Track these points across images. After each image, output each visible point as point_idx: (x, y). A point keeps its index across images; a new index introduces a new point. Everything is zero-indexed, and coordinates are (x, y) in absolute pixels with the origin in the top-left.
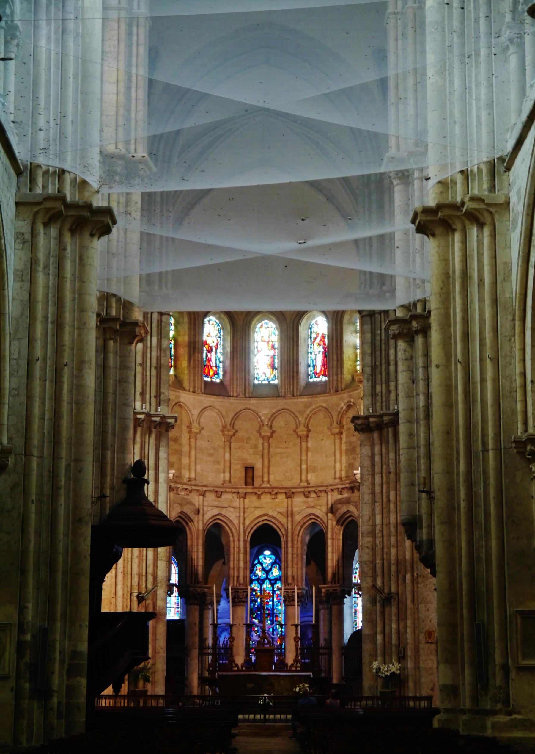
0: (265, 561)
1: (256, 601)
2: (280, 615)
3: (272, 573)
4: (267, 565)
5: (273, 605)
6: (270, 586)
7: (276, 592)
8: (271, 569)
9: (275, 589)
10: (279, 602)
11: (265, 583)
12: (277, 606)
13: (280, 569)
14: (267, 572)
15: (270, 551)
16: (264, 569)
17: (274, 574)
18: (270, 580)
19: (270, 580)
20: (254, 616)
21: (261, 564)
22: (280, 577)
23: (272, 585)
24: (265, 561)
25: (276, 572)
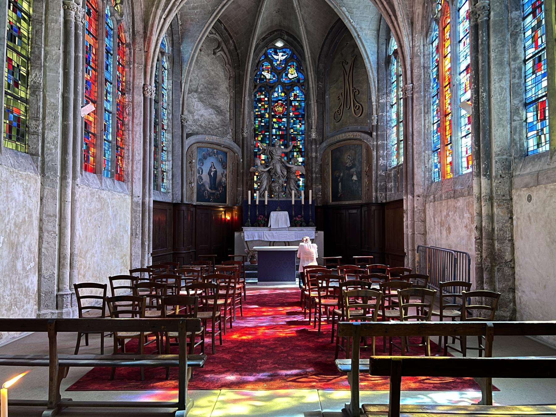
0: (275, 57)
1: (262, 116)
2: (299, 138)
3: (287, 75)
4: (278, 62)
5: (288, 122)
6: (283, 94)
7: (293, 104)
8: (285, 69)
9: (292, 99)
10: (297, 118)
11: (276, 90)
12: (294, 124)
13: (298, 70)
14: (278, 72)
15: (283, 40)
16: (273, 70)
17: (290, 76)
18: (283, 85)
19: (283, 85)
20: (260, 139)
21: (271, 61)
22: (299, 80)
23: (287, 94)
24: (275, 57)
25: (292, 74)
